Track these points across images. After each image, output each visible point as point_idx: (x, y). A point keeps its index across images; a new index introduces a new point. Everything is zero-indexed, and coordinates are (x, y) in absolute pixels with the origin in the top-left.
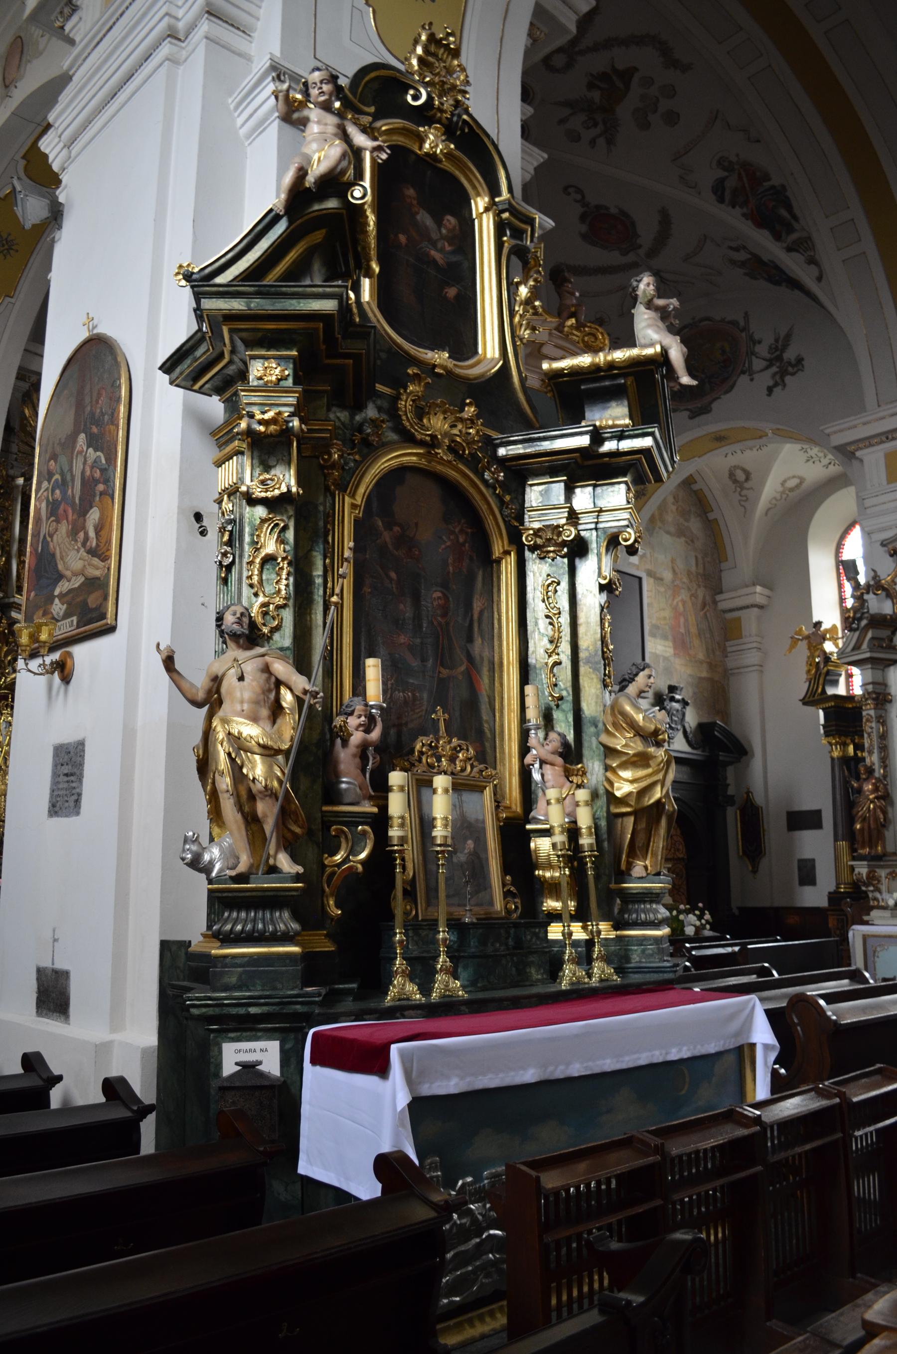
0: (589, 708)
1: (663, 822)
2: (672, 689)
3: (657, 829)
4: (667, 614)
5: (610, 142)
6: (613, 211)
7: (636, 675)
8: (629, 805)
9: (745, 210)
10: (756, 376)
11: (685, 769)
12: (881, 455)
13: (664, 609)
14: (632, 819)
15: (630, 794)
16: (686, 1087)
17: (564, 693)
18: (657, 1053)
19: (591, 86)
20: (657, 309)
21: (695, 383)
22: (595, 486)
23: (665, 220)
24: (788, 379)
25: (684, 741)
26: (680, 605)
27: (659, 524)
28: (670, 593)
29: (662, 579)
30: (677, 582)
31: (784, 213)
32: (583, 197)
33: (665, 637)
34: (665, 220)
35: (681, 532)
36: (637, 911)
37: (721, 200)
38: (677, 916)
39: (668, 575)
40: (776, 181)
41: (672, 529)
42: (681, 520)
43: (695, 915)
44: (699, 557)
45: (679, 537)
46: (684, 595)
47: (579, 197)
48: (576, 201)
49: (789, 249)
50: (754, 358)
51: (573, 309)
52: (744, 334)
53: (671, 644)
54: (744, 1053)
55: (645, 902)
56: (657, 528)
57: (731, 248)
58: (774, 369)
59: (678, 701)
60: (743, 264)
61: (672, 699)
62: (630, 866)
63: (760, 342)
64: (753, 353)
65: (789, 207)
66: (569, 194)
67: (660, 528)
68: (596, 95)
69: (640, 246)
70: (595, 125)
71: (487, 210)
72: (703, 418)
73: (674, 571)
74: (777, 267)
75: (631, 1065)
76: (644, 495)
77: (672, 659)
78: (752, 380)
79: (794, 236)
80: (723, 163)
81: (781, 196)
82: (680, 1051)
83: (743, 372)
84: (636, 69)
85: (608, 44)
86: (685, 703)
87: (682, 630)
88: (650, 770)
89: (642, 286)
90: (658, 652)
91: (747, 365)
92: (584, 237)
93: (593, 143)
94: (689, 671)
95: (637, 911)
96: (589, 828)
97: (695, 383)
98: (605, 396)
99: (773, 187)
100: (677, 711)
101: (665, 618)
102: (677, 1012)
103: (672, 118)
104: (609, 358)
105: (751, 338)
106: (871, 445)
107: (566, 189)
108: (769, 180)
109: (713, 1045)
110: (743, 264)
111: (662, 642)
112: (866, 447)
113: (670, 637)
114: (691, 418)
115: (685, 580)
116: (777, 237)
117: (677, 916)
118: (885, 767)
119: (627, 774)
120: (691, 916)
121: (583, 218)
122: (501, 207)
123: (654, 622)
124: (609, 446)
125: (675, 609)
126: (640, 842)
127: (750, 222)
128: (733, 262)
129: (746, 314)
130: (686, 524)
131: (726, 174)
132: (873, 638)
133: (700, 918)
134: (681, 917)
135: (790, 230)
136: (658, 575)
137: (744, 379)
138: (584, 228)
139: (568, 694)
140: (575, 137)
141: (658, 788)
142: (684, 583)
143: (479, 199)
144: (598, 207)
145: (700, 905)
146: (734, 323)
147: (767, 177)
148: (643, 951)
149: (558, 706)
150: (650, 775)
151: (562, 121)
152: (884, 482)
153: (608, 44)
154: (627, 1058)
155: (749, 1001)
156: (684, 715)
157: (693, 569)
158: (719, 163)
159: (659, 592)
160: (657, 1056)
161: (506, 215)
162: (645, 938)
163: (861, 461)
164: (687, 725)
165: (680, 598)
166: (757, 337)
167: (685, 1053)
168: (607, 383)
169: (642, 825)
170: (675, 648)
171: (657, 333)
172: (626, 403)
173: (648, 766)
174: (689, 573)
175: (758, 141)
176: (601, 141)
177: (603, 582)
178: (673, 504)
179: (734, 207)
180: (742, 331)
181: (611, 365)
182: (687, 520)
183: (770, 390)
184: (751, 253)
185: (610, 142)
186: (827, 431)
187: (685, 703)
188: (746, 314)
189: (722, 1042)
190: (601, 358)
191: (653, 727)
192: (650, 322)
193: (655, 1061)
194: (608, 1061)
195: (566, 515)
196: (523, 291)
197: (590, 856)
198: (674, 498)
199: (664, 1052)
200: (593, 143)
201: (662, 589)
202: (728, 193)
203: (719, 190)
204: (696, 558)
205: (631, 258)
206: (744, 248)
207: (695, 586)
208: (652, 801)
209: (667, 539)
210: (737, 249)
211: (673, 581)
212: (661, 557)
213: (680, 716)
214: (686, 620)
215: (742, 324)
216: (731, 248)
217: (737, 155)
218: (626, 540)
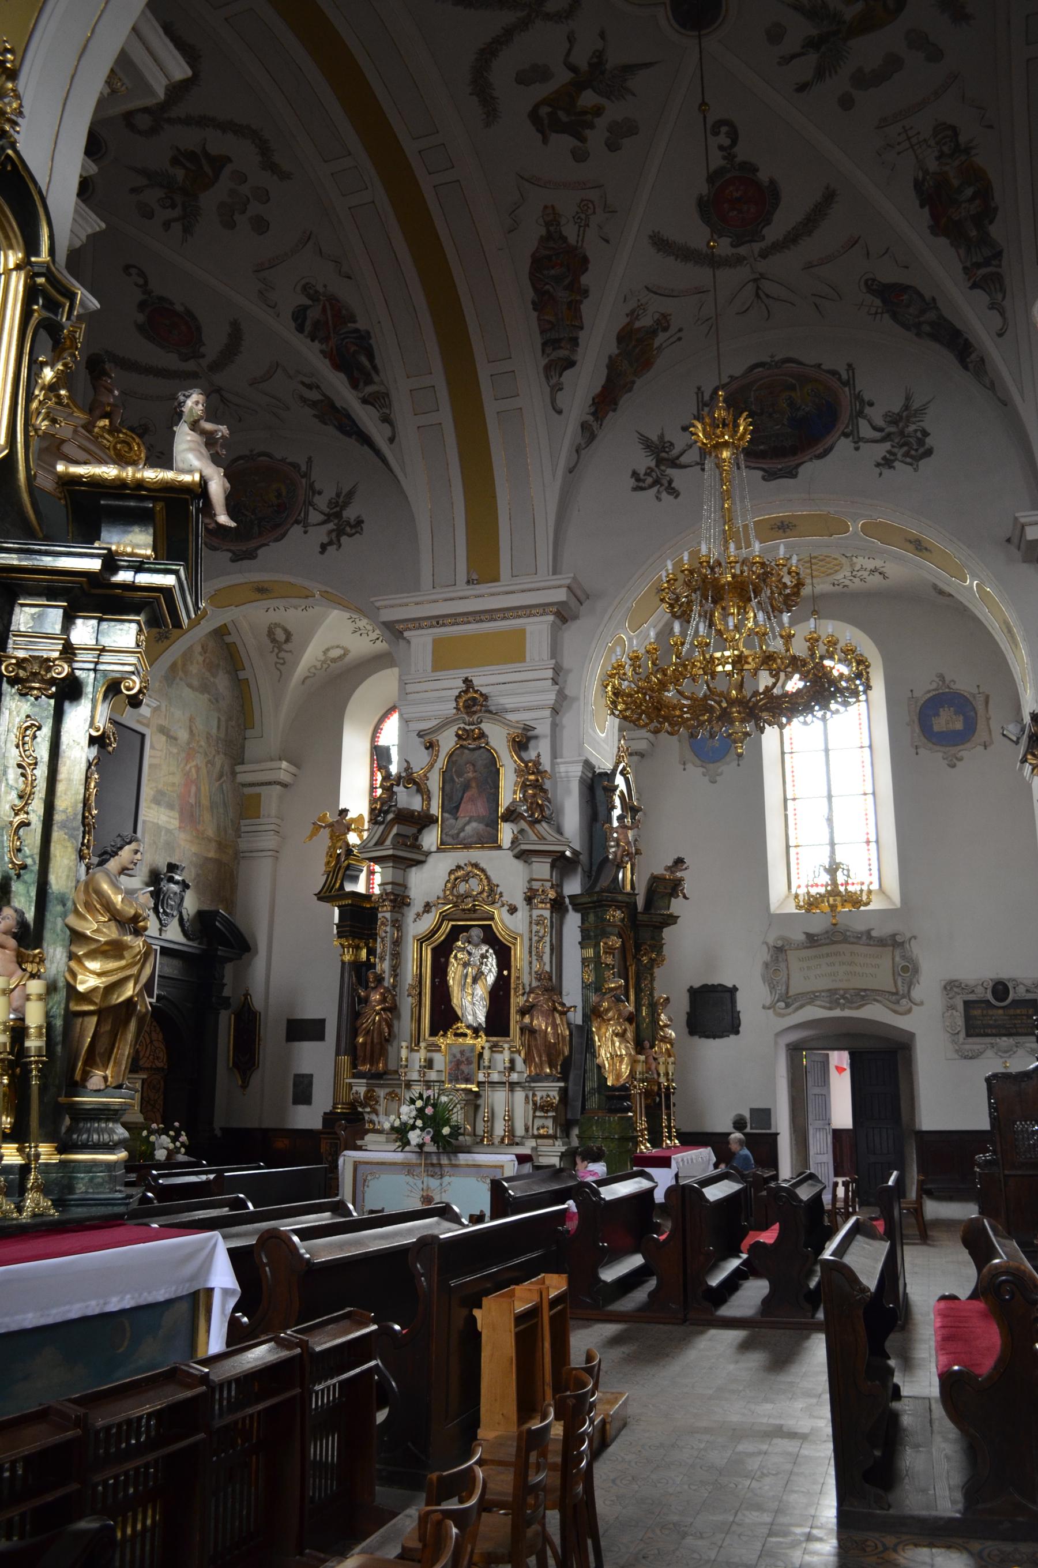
0: (59, 880)
1: (133, 1026)
2: (172, 867)
3: (124, 1033)
4: (177, 779)
5: (187, 230)
6: (179, 308)
7: (121, 848)
8: (93, 1003)
9: (324, 347)
10: (310, 529)
11: (176, 962)
12: (429, 640)
13: (173, 774)
14: (95, 1019)
15: (95, 989)
16: (126, 1344)
17: (29, 861)
18: (93, 1303)
19: (175, 161)
20: (203, 432)
21: (233, 524)
22: (101, 620)
23: (236, 334)
24: (344, 539)
25: (179, 929)
26: (193, 770)
28: (183, 755)
29: (176, 739)
30: (194, 745)
31: (364, 360)
32: (146, 283)
33: (171, 807)
34: (236, 334)
35: (204, 688)
36: (88, 1131)
37: (300, 329)
38: (148, 1136)
39: (183, 735)
40: (361, 325)
41: (195, 683)
42: (207, 674)
43: (168, 1135)
44: (223, 719)
45: (202, 692)
46: (199, 760)
47: (141, 281)
48: (136, 285)
49: (365, 401)
50: (311, 508)
51: (108, 409)
52: (304, 481)
53: (177, 815)
54: (198, 1301)
55: (99, 1120)
56: (178, 680)
57: (303, 383)
58: (331, 526)
59: (177, 883)
60: (314, 404)
61: (171, 880)
62: (86, 1076)
63: (320, 493)
64: (311, 504)
65: (371, 357)
66: (130, 275)
67: (181, 679)
68: (180, 174)
69: (203, 356)
70: (173, 206)
71: (18, 267)
72: (246, 562)
73: (191, 731)
74: (349, 416)
75: (59, 1319)
76: (167, 638)
77: (176, 832)
78: (306, 532)
79: (370, 389)
80: (307, 289)
81: (363, 340)
82: (122, 1299)
83: (297, 522)
84: (229, 160)
85: (202, 121)
86: (185, 886)
87: (192, 801)
88: (123, 963)
89: (189, 403)
90: (160, 823)
91: (302, 515)
92: (140, 328)
93: (167, 225)
94: (194, 849)
95: (88, 1131)
96: (40, 1027)
97: (233, 524)
98: (128, 518)
99: (357, 331)
100: (175, 893)
101: (173, 784)
102: (125, 1252)
103: (260, 225)
104: (139, 475)
105: (311, 486)
106: (420, 628)
107: (127, 268)
108: (355, 322)
109: (163, 1291)
110: (314, 404)
112: (415, 628)
113: (177, 807)
114: (233, 561)
115: (203, 743)
116: (354, 385)
117: (148, 1136)
118: (396, 976)
119: (94, 965)
120: (164, 1137)
121: (142, 306)
122: (36, 269)
123: (160, 786)
124: (124, 576)
125: (187, 774)
126: (101, 1048)
127: (327, 361)
128: (304, 400)
129: (310, 458)
130: (212, 680)
131: (309, 302)
132: (397, 834)
133: (174, 1140)
134: (152, 1138)
135: (369, 381)
136: (172, 733)
137: (296, 530)
138: (141, 318)
139: (33, 863)
140: (150, 215)
141: (131, 985)
142: (201, 746)
143: (10, 253)
144: (161, 299)
145: (177, 1124)
146: (295, 466)
147: (353, 319)
148: (91, 1179)
149: (19, 876)
150: (122, 968)
151: (134, 190)
152: (429, 668)
153: (202, 121)
154: (54, 1311)
155: (210, 1238)
156: (182, 899)
157: (214, 731)
158: (305, 288)
159: (171, 753)
160: (93, 1307)
161: (41, 280)
162: (95, 1163)
163: (409, 642)
164: (184, 912)
165: (194, 763)
166: (317, 486)
167: (128, 1303)
168: (132, 504)
169: (106, 1027)
170: (181, 821)
171: (199, 459)
172: (151, 531)
173: (121, 957)
174: (208, 736)
175: (349, 278)
176: (177, 227)
177: (95, 734)
178: (200, 654)
179: (313, 340)
180: (302, 477)
181: (140, 485)
182: (214, 676)
183: (324, 548)
184: (324, 395)
185: (187, 230)
186: (377, 604)
187: (185, 886)
188: (310, 458)
189: (174, 1288)
190: (129, 473)
191: (132, 912)
192: (192, 445)
193: (90, 1312)
194: (30, 1315)
195: (60, 647)
196: (48, 374)
197: (36, 1062)
198: (203, 647)
199: (102, 1302)
200: (167, 225)
201: (175, 751)
202: (308, 326)
203: (299, 317)
204: (219, 718)
205: (190, 366)
206: (318, 387)
207: (213, 752)
208: (121, 999)
209: (187, 692)
210: (309, 387)
211: (188, 743)
212: (178, 713)
213: (178, 901)
214: (198, 789)
215: (304, 468)
216: (303, 383)
217: (325, 286)
218: (129, 689)
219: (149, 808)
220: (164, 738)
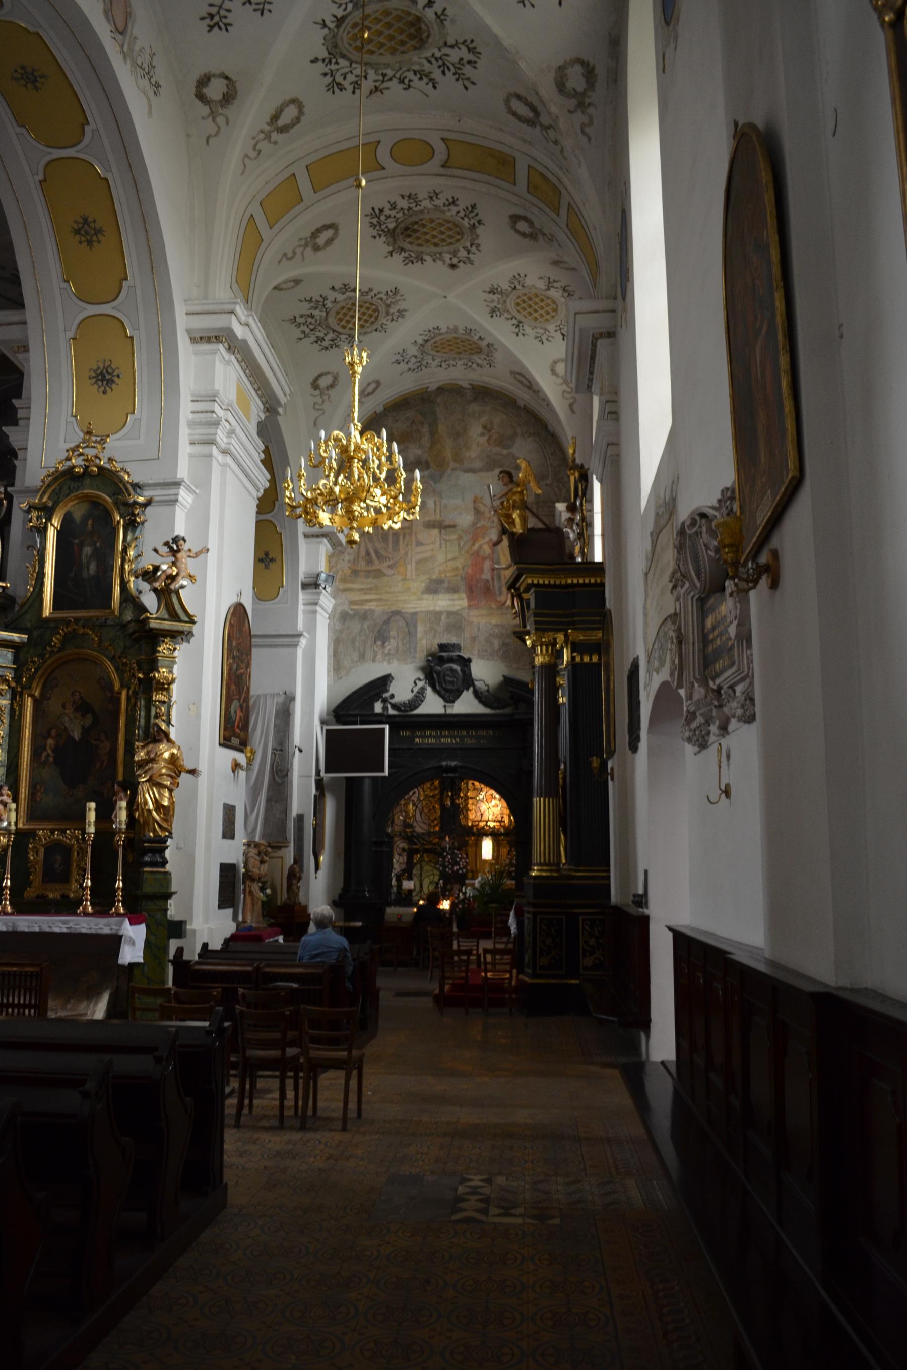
13: (454, 559)
25: (476, 702)
27: (452, 464)
33: (453, 590)
53: (464, 596)
73: (477, 512)
87: (487, 575)
101: (456, 569)
111: (448, 596)
113: (463, 588)
130: (505, 452)
136: (447, 523)
165: (487, 539)
170: (470, 599)
219: (422, 599)
220: (435, 532)
